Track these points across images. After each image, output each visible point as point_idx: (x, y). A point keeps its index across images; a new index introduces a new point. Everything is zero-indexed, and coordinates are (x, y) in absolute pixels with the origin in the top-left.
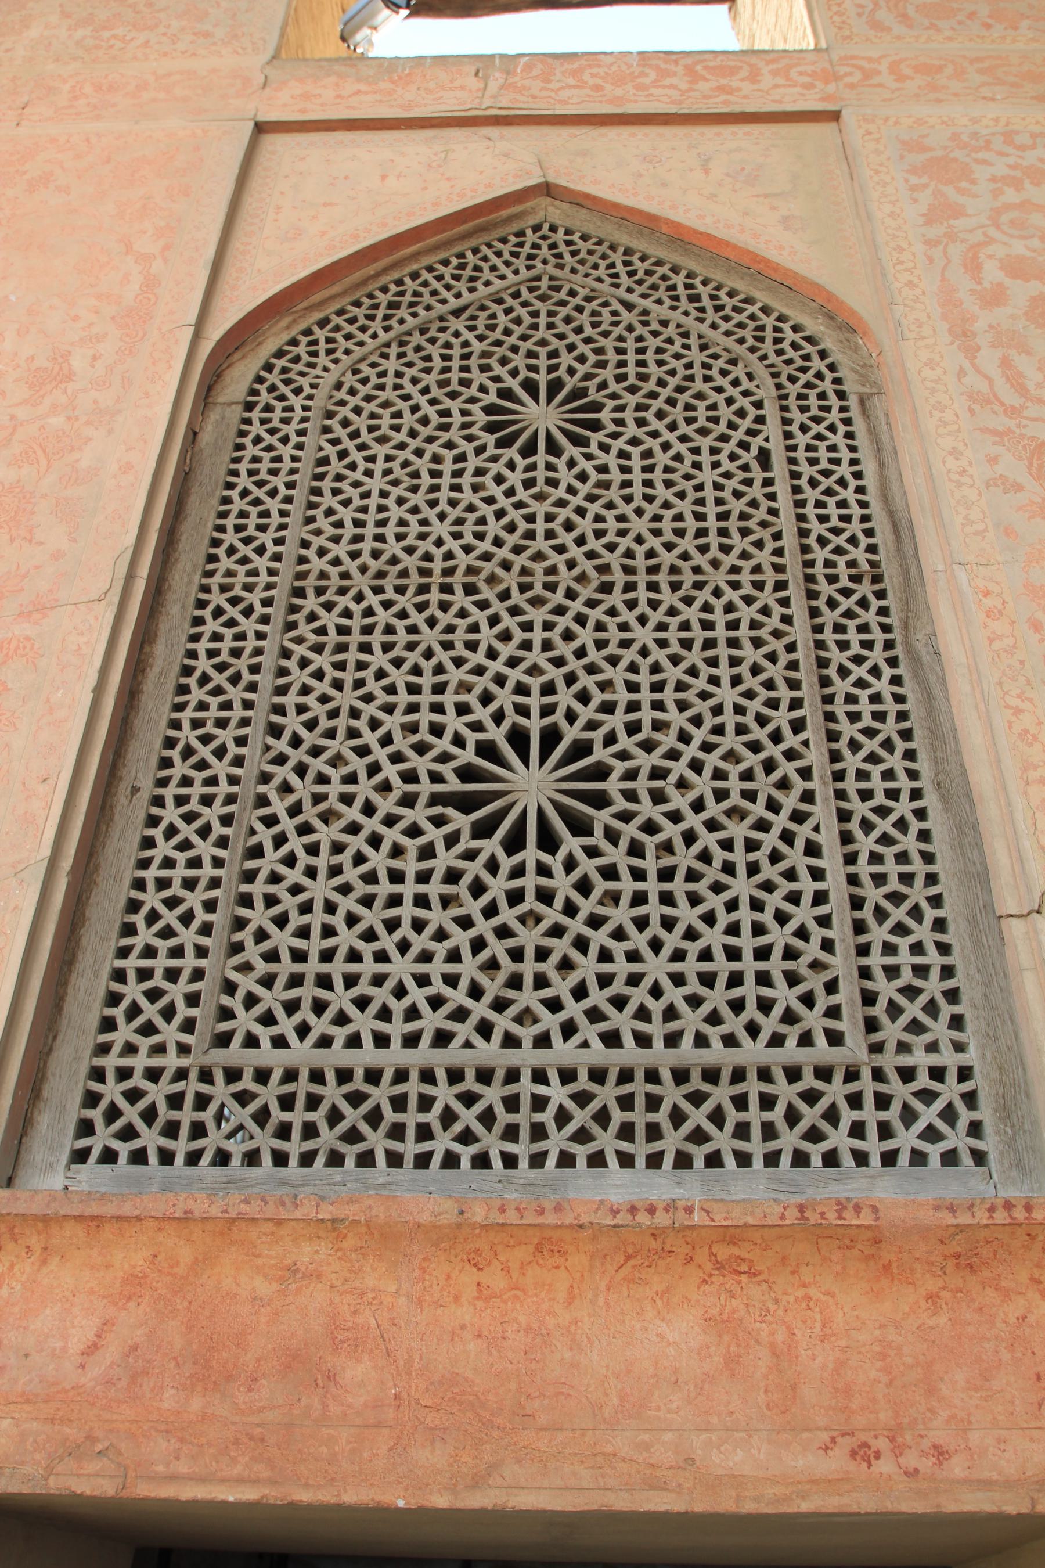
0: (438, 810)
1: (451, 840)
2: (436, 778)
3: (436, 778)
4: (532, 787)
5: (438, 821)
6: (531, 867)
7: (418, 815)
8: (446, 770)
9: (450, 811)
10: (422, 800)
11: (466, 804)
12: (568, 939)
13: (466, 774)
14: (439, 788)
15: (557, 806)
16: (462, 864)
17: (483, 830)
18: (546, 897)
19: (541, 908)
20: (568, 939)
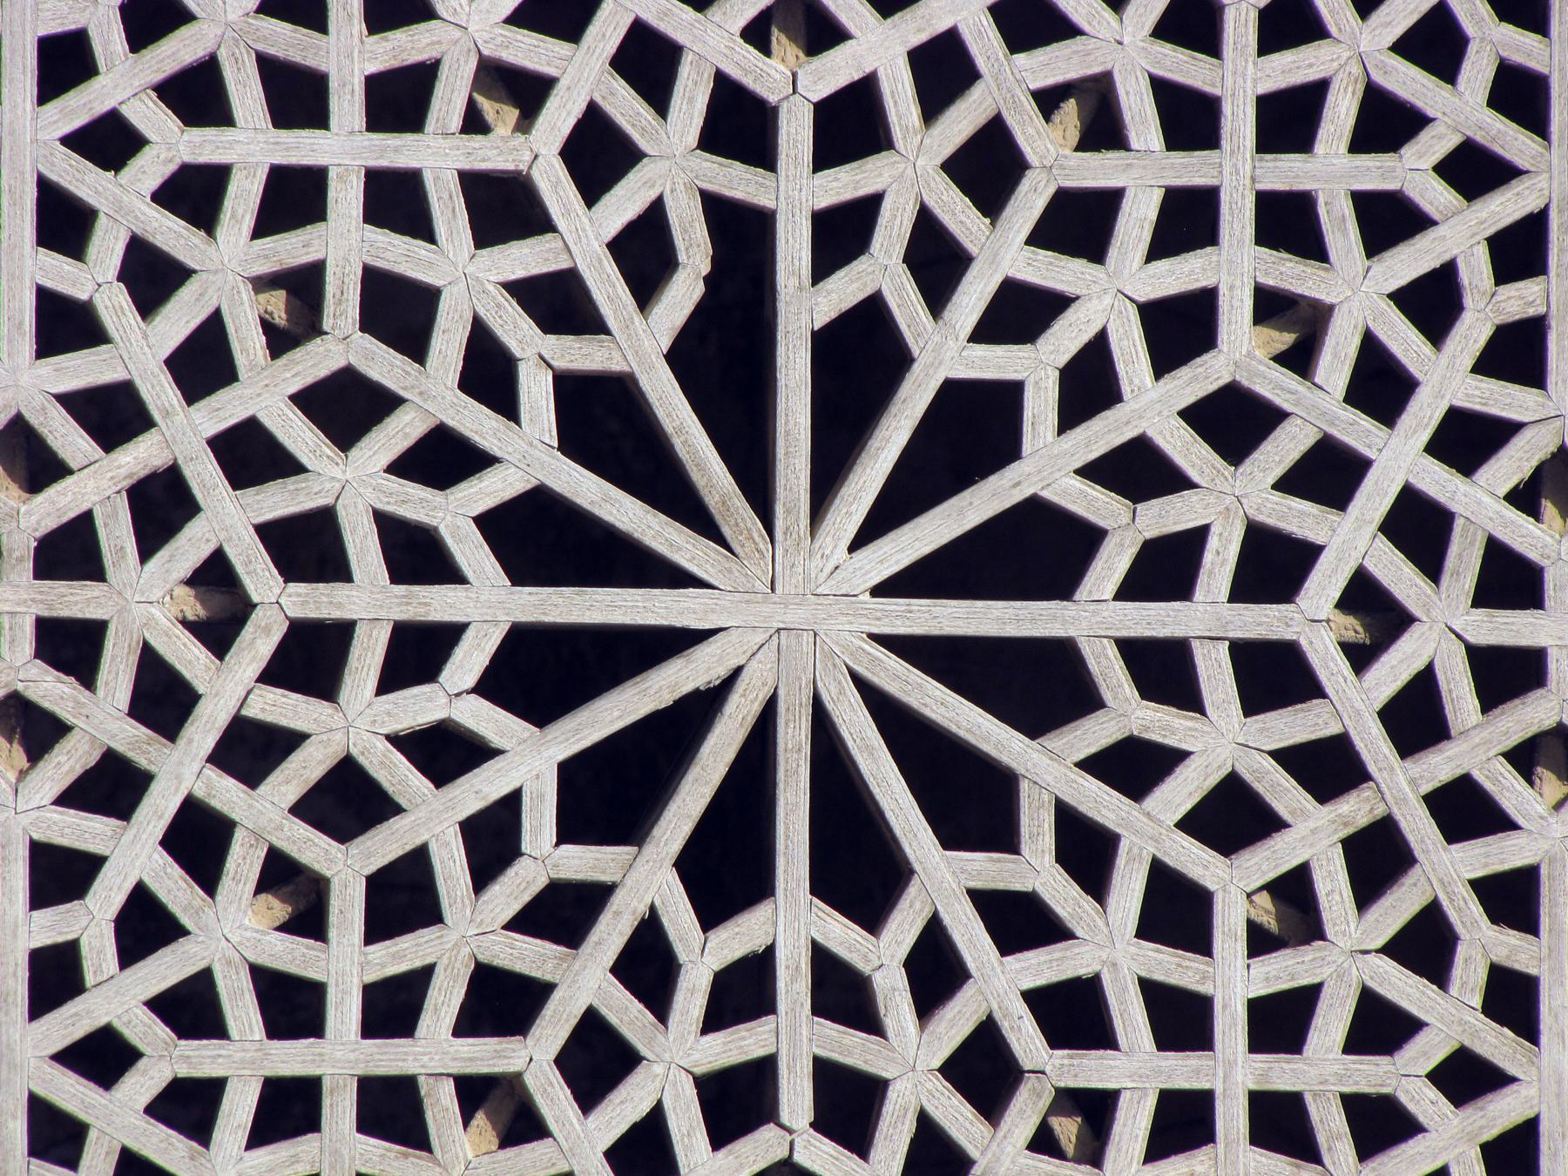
0: (694, 251)
1: (558, 303)
2: (841, 235)
3: (841, 235)
4: (795, 610)
5: (644, 252)
6: (433, 603)
7: (674, 165)
8: (881, 268)
9: (683, 294)
10: (738, 181)
11: (725, 355)
12: (134, 740)
13: (861, 356)
14: (793, 247)
15: (702, 707)
16: (448, 344)
17: (601, 419)
18: (310, 660)
19: (259, 642)
20: (134, 740)
